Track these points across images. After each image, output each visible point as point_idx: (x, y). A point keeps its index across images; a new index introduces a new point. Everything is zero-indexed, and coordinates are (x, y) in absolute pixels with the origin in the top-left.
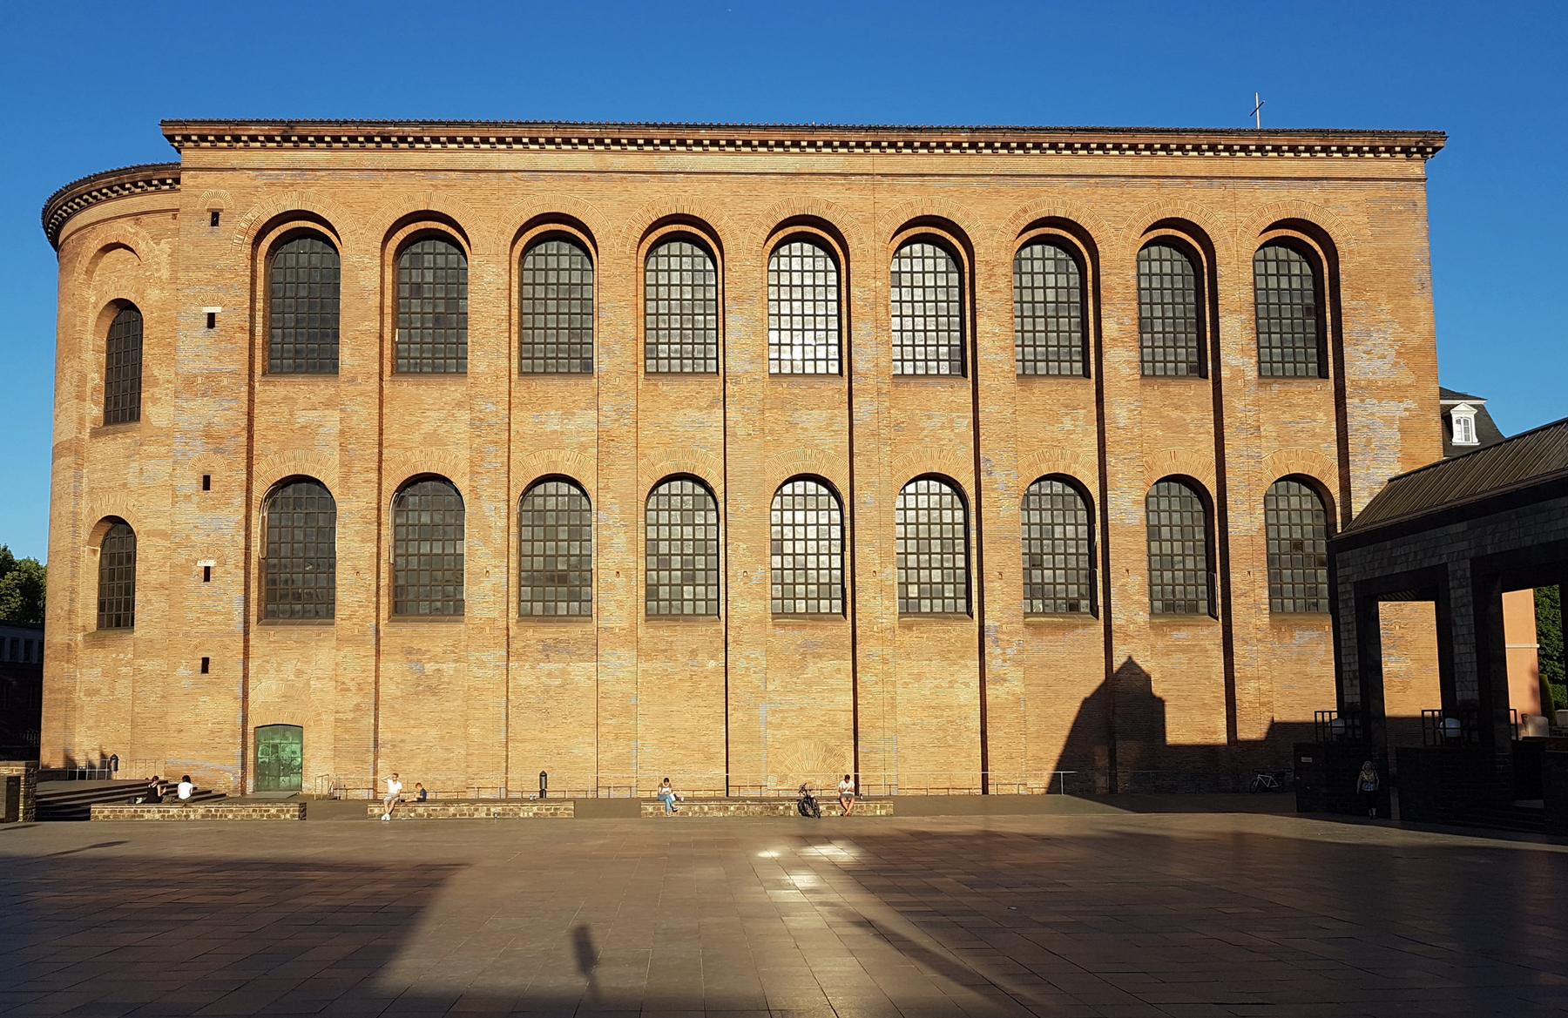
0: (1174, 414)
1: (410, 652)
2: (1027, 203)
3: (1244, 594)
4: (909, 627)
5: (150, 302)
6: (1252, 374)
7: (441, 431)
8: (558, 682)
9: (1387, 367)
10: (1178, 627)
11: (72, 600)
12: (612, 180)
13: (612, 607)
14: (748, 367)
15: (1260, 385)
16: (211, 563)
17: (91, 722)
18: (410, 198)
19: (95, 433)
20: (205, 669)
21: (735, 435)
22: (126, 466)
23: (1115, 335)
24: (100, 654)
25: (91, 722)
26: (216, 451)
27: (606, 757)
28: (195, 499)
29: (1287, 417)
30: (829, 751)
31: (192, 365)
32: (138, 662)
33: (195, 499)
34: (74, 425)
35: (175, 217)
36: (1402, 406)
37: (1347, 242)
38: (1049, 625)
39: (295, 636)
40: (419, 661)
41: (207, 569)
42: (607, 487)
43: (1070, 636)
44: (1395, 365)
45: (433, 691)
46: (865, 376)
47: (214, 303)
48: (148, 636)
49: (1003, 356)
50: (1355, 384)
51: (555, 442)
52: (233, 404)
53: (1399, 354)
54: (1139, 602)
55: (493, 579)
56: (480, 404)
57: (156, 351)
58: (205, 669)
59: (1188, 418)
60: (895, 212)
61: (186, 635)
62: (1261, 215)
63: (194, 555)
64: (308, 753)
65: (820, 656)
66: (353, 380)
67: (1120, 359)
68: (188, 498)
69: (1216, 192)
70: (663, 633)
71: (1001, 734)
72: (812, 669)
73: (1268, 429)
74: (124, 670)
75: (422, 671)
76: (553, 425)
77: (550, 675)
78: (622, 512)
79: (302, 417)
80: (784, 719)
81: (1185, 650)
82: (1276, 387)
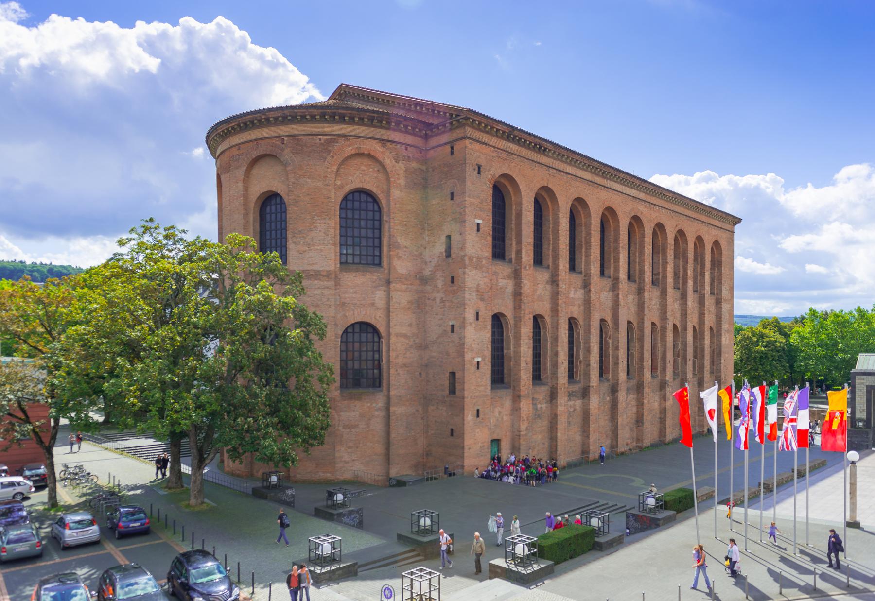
16: (479, 359)
20: (478, 416)
22: (373, 293)
24: (358, 404)
28: (474, 325)
33: (474, 325)
52: (487, 275)
58: (478, 416)
68: (471, 324)
74: (377, 413)
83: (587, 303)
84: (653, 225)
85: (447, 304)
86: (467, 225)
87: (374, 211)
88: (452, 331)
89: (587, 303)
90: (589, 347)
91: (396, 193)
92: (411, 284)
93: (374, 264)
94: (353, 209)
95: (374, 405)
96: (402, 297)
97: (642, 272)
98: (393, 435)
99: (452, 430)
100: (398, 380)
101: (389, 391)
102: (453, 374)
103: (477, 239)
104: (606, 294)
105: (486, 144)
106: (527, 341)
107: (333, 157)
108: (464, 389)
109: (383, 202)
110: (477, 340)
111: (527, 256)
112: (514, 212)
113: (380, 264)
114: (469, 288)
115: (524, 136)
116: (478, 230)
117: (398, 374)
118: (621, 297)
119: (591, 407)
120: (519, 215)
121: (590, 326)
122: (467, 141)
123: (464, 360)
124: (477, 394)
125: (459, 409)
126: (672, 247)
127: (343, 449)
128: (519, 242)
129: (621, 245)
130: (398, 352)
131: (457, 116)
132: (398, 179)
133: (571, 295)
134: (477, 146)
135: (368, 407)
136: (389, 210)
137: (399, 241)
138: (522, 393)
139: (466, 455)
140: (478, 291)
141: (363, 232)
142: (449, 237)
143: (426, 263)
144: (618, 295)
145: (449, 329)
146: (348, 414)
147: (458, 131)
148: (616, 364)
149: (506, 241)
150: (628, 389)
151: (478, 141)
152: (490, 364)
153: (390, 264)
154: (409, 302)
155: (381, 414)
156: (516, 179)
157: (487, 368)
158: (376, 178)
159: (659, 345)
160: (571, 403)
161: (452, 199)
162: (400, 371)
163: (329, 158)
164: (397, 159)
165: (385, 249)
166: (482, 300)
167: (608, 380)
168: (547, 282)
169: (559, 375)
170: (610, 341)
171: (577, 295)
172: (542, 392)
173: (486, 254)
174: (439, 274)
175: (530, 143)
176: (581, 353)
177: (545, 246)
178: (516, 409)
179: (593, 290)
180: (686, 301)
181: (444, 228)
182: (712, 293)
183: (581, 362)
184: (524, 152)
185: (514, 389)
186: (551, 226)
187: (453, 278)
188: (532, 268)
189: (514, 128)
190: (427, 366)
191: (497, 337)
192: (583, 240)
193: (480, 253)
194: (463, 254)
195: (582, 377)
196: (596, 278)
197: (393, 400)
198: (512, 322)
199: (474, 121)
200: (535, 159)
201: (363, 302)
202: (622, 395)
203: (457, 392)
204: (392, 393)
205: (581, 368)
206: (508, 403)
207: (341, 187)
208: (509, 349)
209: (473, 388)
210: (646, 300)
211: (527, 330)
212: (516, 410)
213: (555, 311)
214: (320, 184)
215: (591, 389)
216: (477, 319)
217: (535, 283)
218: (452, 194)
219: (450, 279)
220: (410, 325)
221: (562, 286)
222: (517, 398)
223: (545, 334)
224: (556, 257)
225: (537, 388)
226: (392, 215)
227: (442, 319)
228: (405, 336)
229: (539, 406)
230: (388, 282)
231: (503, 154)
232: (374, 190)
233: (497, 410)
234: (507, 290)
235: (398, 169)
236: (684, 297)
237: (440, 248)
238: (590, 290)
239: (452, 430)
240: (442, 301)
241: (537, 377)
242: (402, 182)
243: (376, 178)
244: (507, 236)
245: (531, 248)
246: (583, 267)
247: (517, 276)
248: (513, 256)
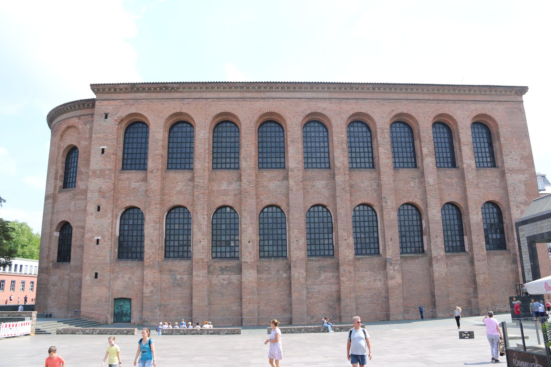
0: (449, 180)
1: (170, 271)
2: (393, 108)
3: (477, 244)
4: (359, 259)
5: (82, 146)
6: (474, 166)
7: (183, 189)
8: (227, 282)
9: (518, 163)
10: (455, 256)
11: (49, 251)
12: (246, 101)
13: (247, 254)
14: (296, 165)
15: (477, 170)
16: (99, 238)
17: (54, 296)
18: (174, 108)
19: (59, 192)
20: (96, 277)
21: (292, 190)
22: (70, 203)
23: (427, 153)
24: (58, 271)
25: (54, 296)
26: (102, 197)
27: (245, 311)
28: (94, 214)
29: (487, 181)
30: (330, 306)
32: (71, 274)
33: (94, 214)
34: (53, 189)
35: (92, 117)
36: (524, 176)
37: (501, 121)
38: (411, 257)
39: (129, 265)
40: (174, 275)
42: (245, 210)
43: (417, 261)
44: (520, 162)
45: (179, 285)
46: (339, 169)
47: (104, 145)
49: (388, 161)
50: (508, 169)
51: (226, 193)
52: (109, 180)
53: (521, 159)
54: (441, 248)
55: (202, 243)
56: (197, 180)
57: (83, 162)
58: (96, 277)
59: (453, 182)
60: (348, 111)
61: (90, 264)
62: (472, 112)
64: (133, 309)
65: (325, 271)
66: (152, 172)
67: (429, 161)
68: (92, 214)
69: (457, 105)
70: (266, 263)
71: (394, 298)
72: (323, 276)
73: (481, 185)
74: (66, 277)
75: (175, 279)
76: (224, 186)
77: (224, 280)
78: (250, 219)
79: (134, 185)
80: (313, 295)
81: (458, 264)
82: (482, 171)
95: (65, 272)
105: (114, 100)
114: (92, 191)
117: (76, 252)
134: (106, 103)
137: (82, 170)
139: (82, 304)
140: (100, 192)
151: (106, 100)
162: (77, 250)
173: (109, 167)
207: (63, 146)
209: (91, 257)
216: (99, 210)
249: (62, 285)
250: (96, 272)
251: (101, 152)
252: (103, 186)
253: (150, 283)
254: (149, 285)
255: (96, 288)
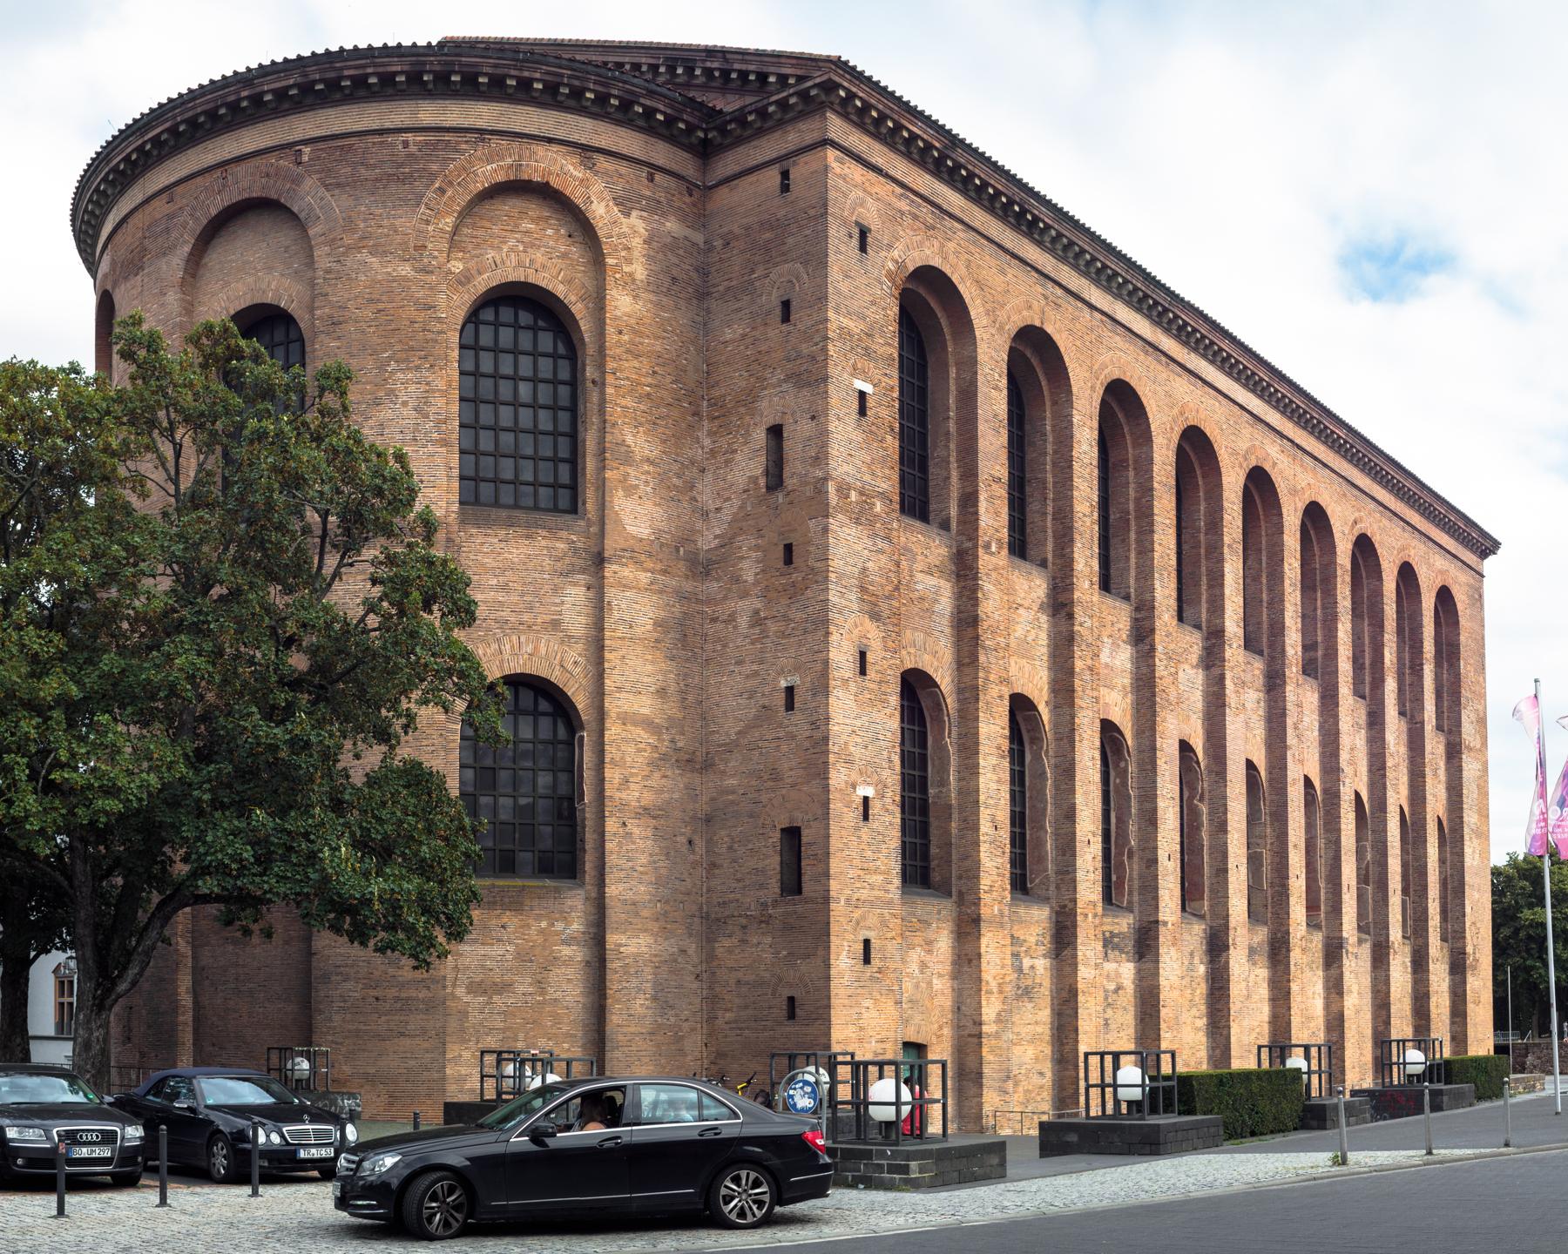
16: (869, 792)
20: (867, 960)
22: (556, 590)
24: (511, 920)
28: (852, 685)
31: (846, 468)
33: (852, 685)
41: (866, 799)
48: (629, 895)
57: (628, 402)
58: (867, 960)
63: (854, 776)
74: (566, 951)
83: (1145, 687)
84: (1301, 506)
85: (773, 627)
86: (831, 389)
87: (554, 356)
88: (790, 706)
89: (1145, 687)
90: (1155, 810)
91: (621, 303)
92: (664, 572)
93: (556, 509)
94: (496, 350)
95: (559, 926)
96: (636, 605)
97: (1278, 629)
98: (615, 1018)
99: (791, 1000)
100: (631, 853)
101: (601, 883)
102: (792, 834)
103: (857, 436)
104: (1192, 672)
106: (993, 760)
107: (442, 191)
108: (827, 875)
109: (584, 326)
110: (862, 728)
111: (993, 516)
112: (953, 387)
113: (574, 509)
114: (841, 576)
115: (981, 171)
116: (862, 411)
118: (1229, 683)
119: (1163, 982)
120: (969, 396)
121: (1154, 749)
122: (832, 154)
123: (826, 789)
124: (864, 894)
125: (814, 935)
126: (1348, 579)
127: (466, 1054)
128: (970, 473)
129: (1227, 540)
130: (630, 770)
131: (801, 79)
132: (629, 261)
133: (1105, 657)
135: (542, 932)
136: (601, 349)
137: (629, 440)
138: (985, 912)
140: (863, 589)
141: (525, 416)
142: (776, 432)
143: (705, 515)
144: (1222, 678)
145: (780, 700)
146: (482, 950)
147: (802, 126)
148: (1222, 871)
149: (932, 470)
150: (1252, 951)
152: (897, 811)
153: (602, 506)
154: (657, 624)
155: (574, 954)
156: (961, 288)
157: (888, 819)
158: (564, 256)
159: (1321, 843)
160: (1110, 966)
161: (786, 318)
162: (635, 828)
163: (430, 194)
164: (625, 204)
165: (590, 464)
166: (875, 616)
167: (1202, 917)
168: (1041, 607)
169: (1080, 875)
170: (1204, 809)
171: (1118, 659)
172: (1036, 920)
173: (884, 486)
174: (746, 543)
175: (998, 193)
176: (1132, 828)
177: (1033, 506)
178: (966, 961)
179: (1159, 648)
180: (1383, 731)
181: (764, 404)
182: (1439, 728)
183: (1130, 856)
184: (979, 217)
185: (961, 902)
186: (1050, 448)
187: (788, 549)
188: (1005, 552)
189: (954, 141)
190: (708, 820)
191: (908, 747)
192: (1132, 506)
193: (867, 478)
194: (820, 474)
195: (1136, 898)
196: (1166, 617)
197: (614, 915)
198: (951, 702)
199: (851, 96)
200: (1008, 245)
201: (526, 617)
202: (1238, 961)
203: (807, 886)
204: (612, 890)
205: (1133, 869)
206: (944, 943)
208: (944, 782)
209: (852, 873)
210: (1289, 706)
211: (993, 729)
212: (966, 961)
213: (1063, 688)
214: (406, 270)
215: (1162, 929)
216: (863, 672)
217: (1014, 597)
218: (786, 305)
219: (779, 552)
220: (662, 692)
221: (1084, 623)
222: (968, 927)
223: (1037, 758)
224: (1065, 537)
225: (1022, 911)
226: (611, 365)
227: (756, 674)
228: (647, 724)
229: (1027, 962)
230: (599, 560)
231: (925, 209)
232: (560, 290)
233: (915, 955)
234: (937, 608)
235: (629, 233)
236: (1375, 721)
237: (749, 465)
238: (1153, 649)
239: (791, 1000)
240: (757, 620)
241: (1021, 884)
242: (639, 270)
243: (564, 256)
244: (935, 454)
245: (1002, 492)
246: (1132, 582)
247: (964, 570)
248: (954, 512)
249: (543, 992)
250: (870, 935)
251: (855, 405)
252: (870, 565)
253: (993, 985)
254: (989, 992)
255: (868, 1003)
